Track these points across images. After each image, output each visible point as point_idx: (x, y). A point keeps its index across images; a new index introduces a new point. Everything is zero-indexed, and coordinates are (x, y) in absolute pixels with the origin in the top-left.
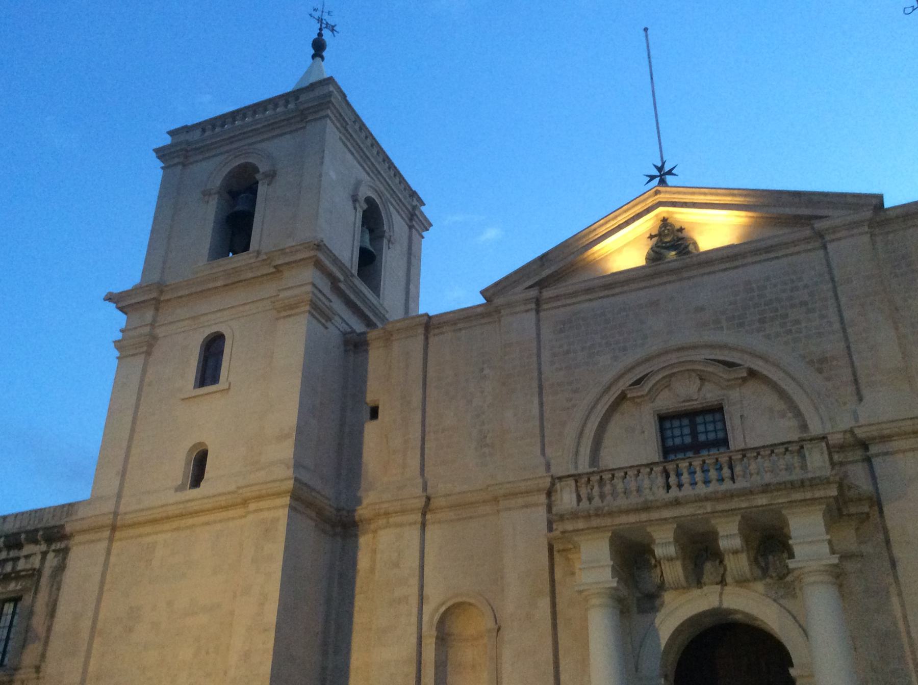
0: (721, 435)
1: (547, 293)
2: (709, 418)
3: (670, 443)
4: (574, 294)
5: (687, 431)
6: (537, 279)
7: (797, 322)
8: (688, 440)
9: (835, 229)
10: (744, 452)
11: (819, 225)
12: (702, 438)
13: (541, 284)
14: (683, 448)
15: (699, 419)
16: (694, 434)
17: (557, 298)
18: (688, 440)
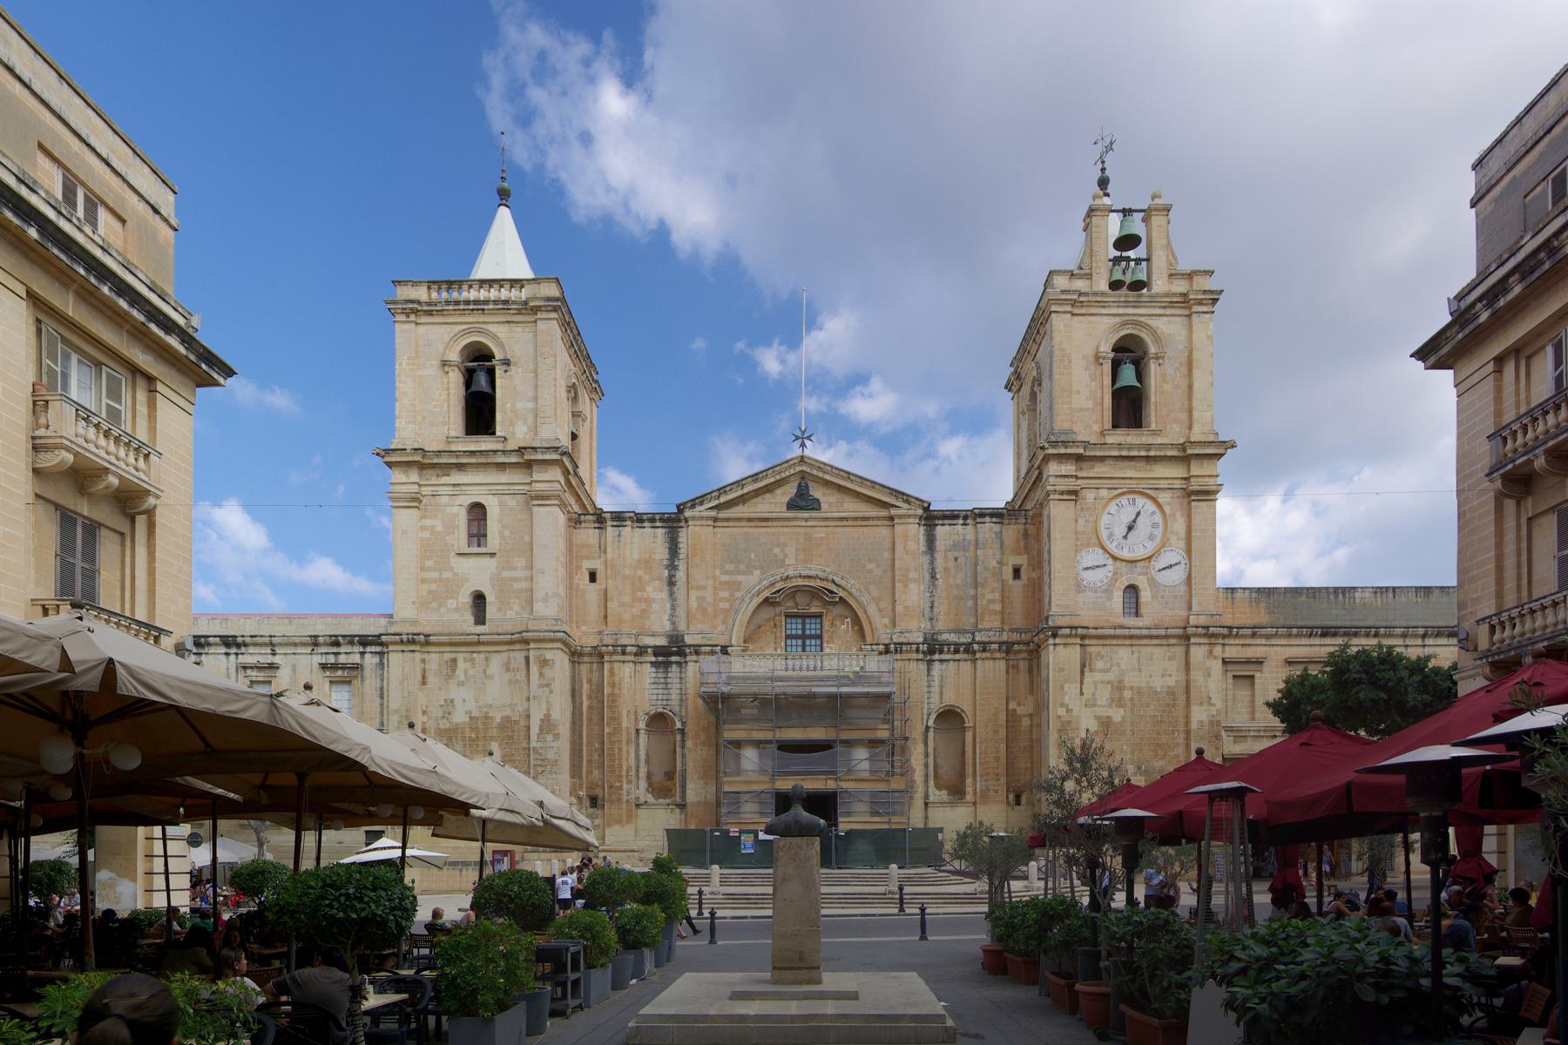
0: (818, 632)
1: (722, 515)
2: (813, 621)
3: (789, 632)
4: (740, 519)
5: (800, 626)
6: (717, 502)
7: (870, 571)
8: (800, 632)
9: (900, 517)
10: (829, 655)
11: (893, 512)
12: (808, 632)
13: (717, 507)
14: (796, 637)
15: (808, 621)
16: (804, 629)
17: (728, 520)
18: (800, 632)
